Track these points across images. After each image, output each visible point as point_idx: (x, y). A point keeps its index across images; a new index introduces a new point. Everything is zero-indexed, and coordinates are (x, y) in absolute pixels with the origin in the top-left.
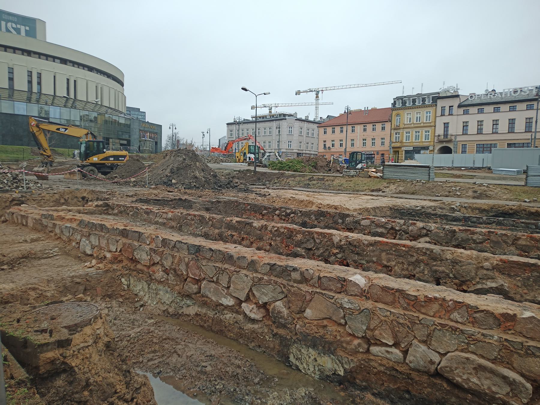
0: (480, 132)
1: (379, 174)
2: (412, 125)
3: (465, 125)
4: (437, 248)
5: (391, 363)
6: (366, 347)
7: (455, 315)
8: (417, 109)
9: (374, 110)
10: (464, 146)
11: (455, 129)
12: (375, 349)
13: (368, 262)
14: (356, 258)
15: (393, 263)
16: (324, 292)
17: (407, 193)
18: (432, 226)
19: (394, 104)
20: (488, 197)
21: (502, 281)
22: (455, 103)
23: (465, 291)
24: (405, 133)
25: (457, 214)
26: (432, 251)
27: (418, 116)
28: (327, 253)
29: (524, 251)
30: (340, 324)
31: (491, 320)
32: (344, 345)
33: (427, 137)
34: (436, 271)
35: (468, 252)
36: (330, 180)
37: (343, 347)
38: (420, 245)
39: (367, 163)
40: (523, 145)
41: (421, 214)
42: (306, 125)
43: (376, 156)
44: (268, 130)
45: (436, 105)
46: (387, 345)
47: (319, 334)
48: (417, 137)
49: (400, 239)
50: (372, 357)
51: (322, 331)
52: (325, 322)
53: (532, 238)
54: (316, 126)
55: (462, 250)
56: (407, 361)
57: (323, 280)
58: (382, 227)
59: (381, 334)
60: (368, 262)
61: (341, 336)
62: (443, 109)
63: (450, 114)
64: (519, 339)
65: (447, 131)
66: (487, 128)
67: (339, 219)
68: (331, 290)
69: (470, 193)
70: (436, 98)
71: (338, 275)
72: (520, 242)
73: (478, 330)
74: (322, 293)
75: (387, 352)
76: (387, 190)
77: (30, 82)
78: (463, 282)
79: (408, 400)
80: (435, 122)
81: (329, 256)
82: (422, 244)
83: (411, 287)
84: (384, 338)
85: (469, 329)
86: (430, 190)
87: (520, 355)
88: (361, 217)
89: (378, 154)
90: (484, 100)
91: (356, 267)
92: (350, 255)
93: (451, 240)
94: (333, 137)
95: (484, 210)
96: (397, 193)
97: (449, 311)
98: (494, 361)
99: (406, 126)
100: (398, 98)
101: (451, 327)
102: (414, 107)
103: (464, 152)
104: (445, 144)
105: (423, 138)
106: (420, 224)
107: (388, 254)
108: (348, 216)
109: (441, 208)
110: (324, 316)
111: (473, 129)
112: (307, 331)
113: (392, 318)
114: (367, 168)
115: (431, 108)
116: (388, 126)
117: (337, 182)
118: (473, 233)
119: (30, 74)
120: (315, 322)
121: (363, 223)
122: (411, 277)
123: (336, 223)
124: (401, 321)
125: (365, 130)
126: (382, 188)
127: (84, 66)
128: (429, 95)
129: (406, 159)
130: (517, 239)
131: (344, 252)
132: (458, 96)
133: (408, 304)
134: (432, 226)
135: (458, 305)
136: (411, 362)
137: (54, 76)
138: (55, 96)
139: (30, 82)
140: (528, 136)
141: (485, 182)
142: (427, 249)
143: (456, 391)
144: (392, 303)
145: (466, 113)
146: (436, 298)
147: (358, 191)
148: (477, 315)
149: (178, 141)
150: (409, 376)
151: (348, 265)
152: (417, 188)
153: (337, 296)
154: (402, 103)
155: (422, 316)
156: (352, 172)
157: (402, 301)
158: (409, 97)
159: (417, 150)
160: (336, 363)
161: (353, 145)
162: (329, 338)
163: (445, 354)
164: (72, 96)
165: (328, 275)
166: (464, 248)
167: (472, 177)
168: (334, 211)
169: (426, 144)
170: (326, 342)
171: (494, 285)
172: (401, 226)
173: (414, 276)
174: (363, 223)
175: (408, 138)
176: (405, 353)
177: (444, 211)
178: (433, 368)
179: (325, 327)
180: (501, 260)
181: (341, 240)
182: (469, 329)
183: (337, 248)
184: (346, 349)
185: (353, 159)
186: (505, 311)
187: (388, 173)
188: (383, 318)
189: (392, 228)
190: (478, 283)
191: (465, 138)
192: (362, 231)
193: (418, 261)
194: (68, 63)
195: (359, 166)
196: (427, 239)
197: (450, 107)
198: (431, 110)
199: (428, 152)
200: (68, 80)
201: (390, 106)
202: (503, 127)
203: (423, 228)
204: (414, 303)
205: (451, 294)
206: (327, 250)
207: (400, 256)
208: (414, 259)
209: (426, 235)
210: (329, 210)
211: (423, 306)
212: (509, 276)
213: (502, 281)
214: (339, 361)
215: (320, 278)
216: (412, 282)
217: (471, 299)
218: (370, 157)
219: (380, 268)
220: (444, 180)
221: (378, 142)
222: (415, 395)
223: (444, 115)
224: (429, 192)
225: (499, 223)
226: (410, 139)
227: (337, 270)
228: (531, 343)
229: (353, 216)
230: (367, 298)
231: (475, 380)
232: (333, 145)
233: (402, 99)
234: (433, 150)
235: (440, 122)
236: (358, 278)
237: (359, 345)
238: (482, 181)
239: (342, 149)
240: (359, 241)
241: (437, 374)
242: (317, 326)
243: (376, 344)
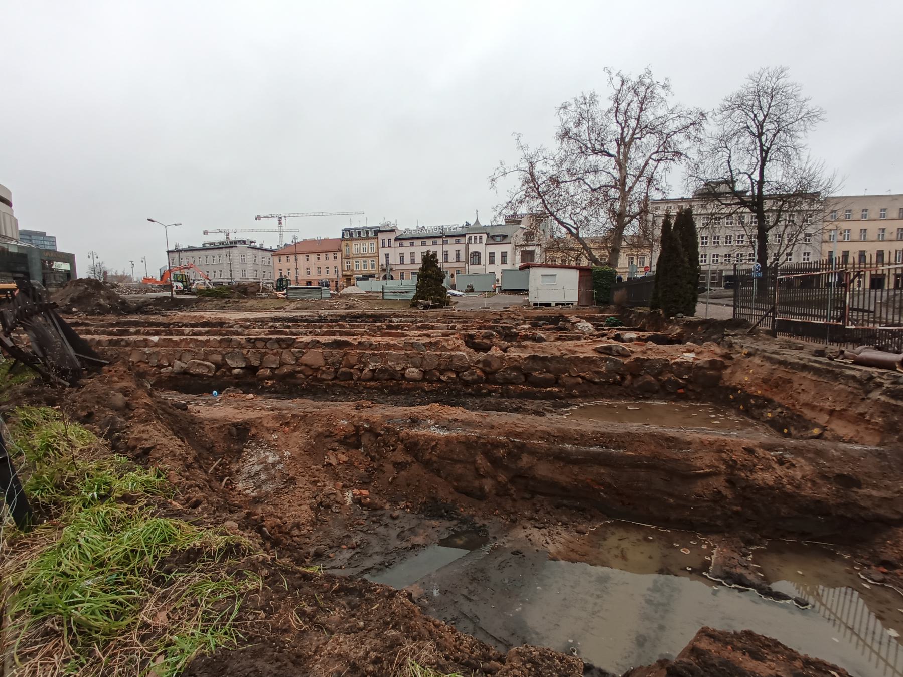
9: (327, 240)
10: (402, 275)
11: (394, 260)
22: (392, 236)
33: (373, 266)
42: (260, 253)
44: (217, 258)
48: (365, 266)
54: (269, 254)
62: (383, 242)
63: (390, 246)
70: (377, 232)
90: (414, 235)
94: (288, 265)
100: (346, 230)
111: (407, 259)
116: (338, 255)
125: (318, 259)
128: (371, 228)
145: (401, 245)
149: (105, 273)
158: (355, 229)
175: (357, 266)
198: (374, 241)
221: (332, 270)
226: (360, 267)
232: (289, 274)
235: (382, 252)
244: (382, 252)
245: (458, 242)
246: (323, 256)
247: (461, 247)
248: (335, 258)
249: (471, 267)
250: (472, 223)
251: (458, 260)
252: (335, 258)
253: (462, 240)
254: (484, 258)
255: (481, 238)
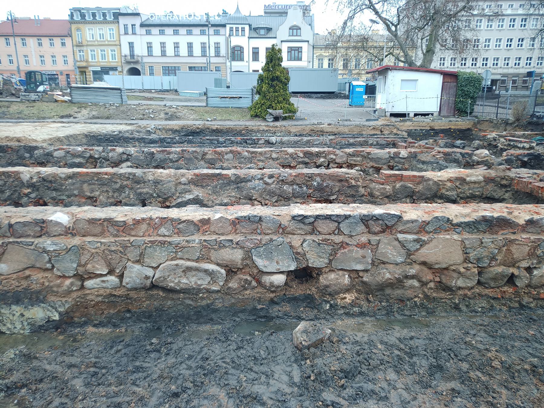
0: (164, 54)
1: (67, 98)
2: (96, 43)
3: (150, 47)
4: (138, 172)
5: (108, 291)
6: (79, 283)
7: (163, 231)
8: (98, 25)
9: (47, 21)
10: (151, 68)
11: (140, 50)
12: (89, 283)
13: (69, 197)
14: (54, 194)
15: (97, 193)
16: (19, 240)
17: (102, 118)
18: (132, 150)
19: (72, 15)
20: (178, 118)
21: (198, 192)
22: (137, 21)
23: (168, 207)
24: (89, 51)
25: (153, 136)
26: (134, 175)
27: (101, 32)
28: (16, 195)
29: (211, 164)
30: (46, 270)
31: (192, 228)
32: (55, 289)
33: (113, 57)
34: (141, 194)
35: (167, 171)
36: (4, 106)
37: (53, 291)
38: (122, 171)
39: (50, 85)
40: (201, 69)
41: (119, 139)
43: (60, 77)
45: (118, 22)
46: (101, 275)
47: (22, 287)
48: (103, 57)
49: (101, 167)
50: (88, 292)
51: (25, 284)
52: (27, 272)
53: (216, 152)
55: (161, 170)
56: (124, 284)
57: (16, 227)
58: (79, 156)
59: (93, 267)
60: (69, 197)
61: (49, 281)
62: (126, 27)
63: (134, 33)
64: (214, 237)
65: (133, 51)
66: (170, 51)
67: (26, 153)
68: (28, 236)
69: (162, 115)
71: (35, 217)
72: (208, 157)
73: (182, 238)
74: (17, 242)
75: (103, 281)
76: (79, 115)
78: (166, 199)
79: (130, 318)
80: (120, 41)
81: (20, 197)
82: (124, 169)
83: (119, 213)
84: (98, 269)
85: (176, 239)
86: (123, 113)
87: (215, 250)
88: (52, 148)
89: (62, 74)
90: (164, 20)
91: (56, 204)
92: (46, 193)
93: (151, 162)
95: (176, 131)
96: (91, 119)
97: (156, 228)
98: (197, 261)
99: (89, 43)
101: (160, 242)
102: (94, 22)
103: (152, 74)
104: (132, 66)
105: (110, 58)
106: (120, 150)
107: (90, 184)
108: (36, 148)
109: (138, 132)
110: (25, 266)
111: (156, 51)
112: (5, 288)
113: (103, 248)
114: (52, 90)
115: (113, 25)
116: (68, 41)
117: (14, 108)
118: (169, 153)
120: (14, 276)
121: (56, 154)
122: (118, 203)
123: (22, 158)
124: (113, 248)
125: (40, 44)
126: (72, 113)
129: (95, 80)
130: (205, 154)
131: (38, 190)
132: (138, 14)
133: (118, 231)
134: (132, 150)
135: (164, 220)
136: (127, 284)
140: (204, 60)
141: (174, 104)
142: (130, 174)
143: (171, 295)
144: (102, 234)
145: (148, 33)
146: (143, 219)
147: (44, 118)
148: (181, 226)
150: (127, 297)
151: (45, 204)
152: (111, 111)
153: (36, 241)
154: (81, 15)
155: (132, 239)
156: (33, 96)
157: (111, 229)
159: (106, 70)
160: (48, 310)
161: (27, 62)
162: (35, 287)
163: (158, 267)
165: (22, 220)
166: (163, 168)
167: (162, 99)
168: (17, 144)
169: (113, 65)
170: (32, 293)
171: (191, 197)
172: (100, 153)
173: (121, 202)
174: (56, 154)
175: (93, 57)
176: (121, 277)
177: (141, 134)
178: (148, 282)
179: (29, 276)
180: (195, 174)
181: (31, 178)
182: (176, 239)
183: (28, 187)
184: (57, 292)
185: (31, 79)
186: (201, 217)
187: (78, 97)
188: (94, 250)
189: (91, 157)
190: (178, 197)
191: (150, 60)
192: (57, 163)
193: (122, 187)
195: (41, 88)
196: (129, 164)
197: (132, 25)
198: (114, 27)
199: (117, 73)
201: (67, 18)
202: (183, 50)
203: (123, 153)
204: (123, 228)
205: (155, 212)
206: (15, 191)
207: (103, 185)
208: (118, 186)
209: (127, 160)
210: (9, 144)
211: (133, 229)
212: (202, 186)
213: (198, 192)
214: (52, 306)
215: (10, 226)
216: (119, 208)
217: (174, 213)
218: (53, 78)
219: (84, 200)
220: (136, 102)
221: (60, 60)
222: (135, 312)
223: (128, 34)
224: (124, 116)
225: (190, 142)
226: (96, 59)
227: (33, 213)
228: (222, 238)
229: (42, 148)
230: (74, 235)
231: (184, 281)
233: (80, 11)
234: (122, 72)
235: (125, 40)
236: (60, 216)
237: (72, 284)
238: (171, 102)
239: (14, 67)
240: (55, 175)
241: (153, 286)
242: (18, 279)
243: (90, 278)
244: (125, 40)
245: (217, 33)
246: (45, 41)
247: (221, 39)
248: (63, 44)
249: (234, 63)
250: (231, 11)
251: (217, 55)
252: (63, 44)
253: (222, 30)
254: (248, 54)
255: (243, 30)
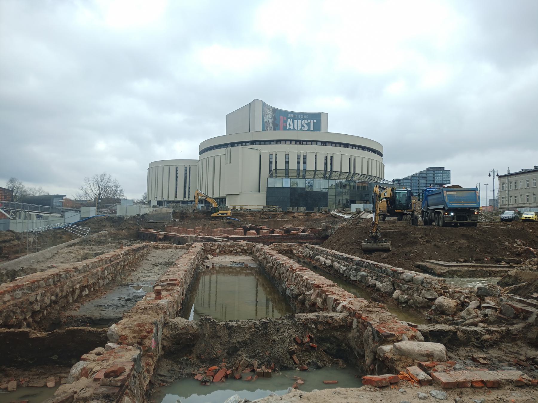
77: (299, 163)
119: (299, 157)
127: (340, 144)
137: (316, 156)
138: (316, 170)
139: (299, 163)
164: (329, 169)
194: (327, 144)
200: (326, 157)
